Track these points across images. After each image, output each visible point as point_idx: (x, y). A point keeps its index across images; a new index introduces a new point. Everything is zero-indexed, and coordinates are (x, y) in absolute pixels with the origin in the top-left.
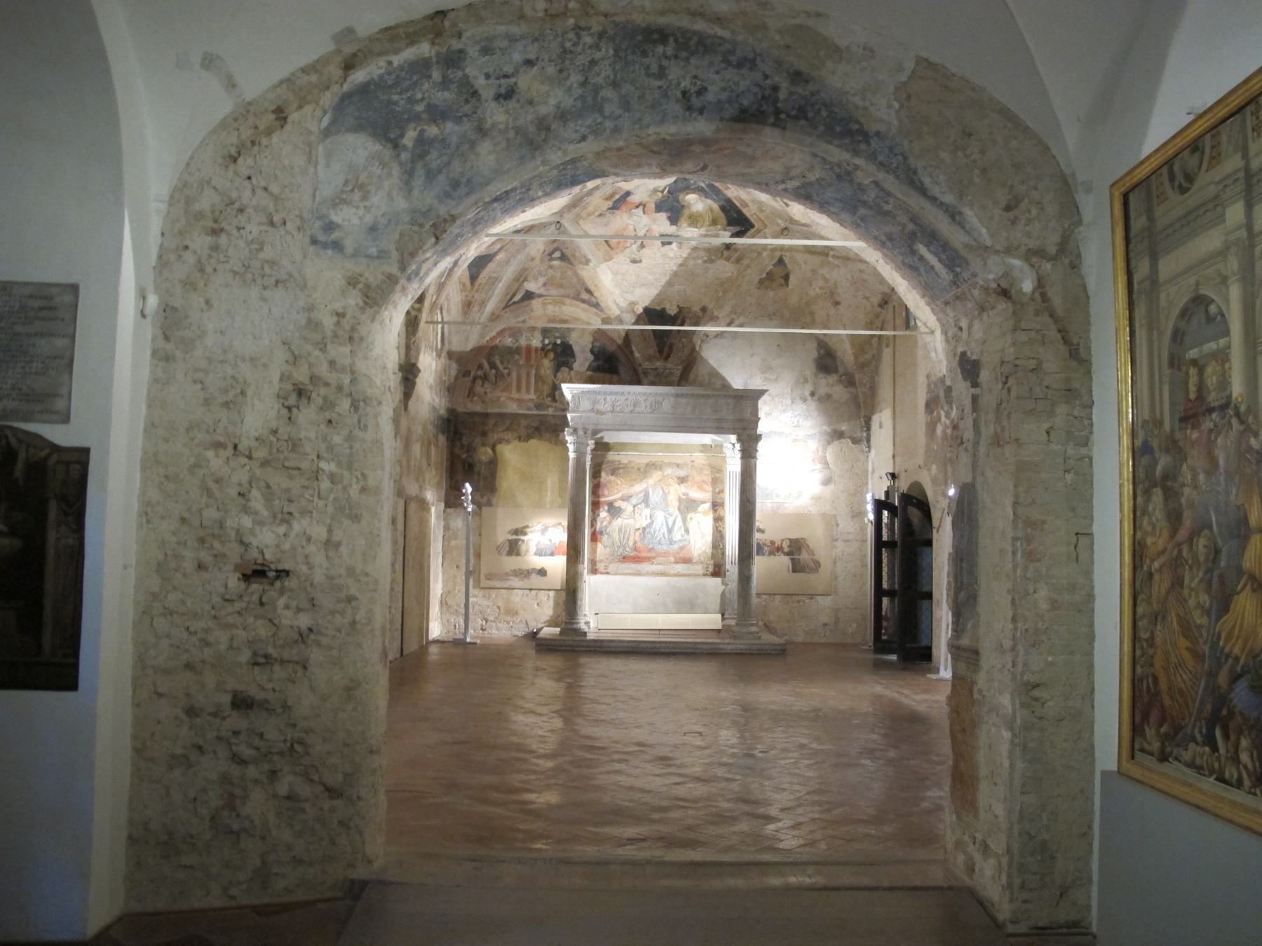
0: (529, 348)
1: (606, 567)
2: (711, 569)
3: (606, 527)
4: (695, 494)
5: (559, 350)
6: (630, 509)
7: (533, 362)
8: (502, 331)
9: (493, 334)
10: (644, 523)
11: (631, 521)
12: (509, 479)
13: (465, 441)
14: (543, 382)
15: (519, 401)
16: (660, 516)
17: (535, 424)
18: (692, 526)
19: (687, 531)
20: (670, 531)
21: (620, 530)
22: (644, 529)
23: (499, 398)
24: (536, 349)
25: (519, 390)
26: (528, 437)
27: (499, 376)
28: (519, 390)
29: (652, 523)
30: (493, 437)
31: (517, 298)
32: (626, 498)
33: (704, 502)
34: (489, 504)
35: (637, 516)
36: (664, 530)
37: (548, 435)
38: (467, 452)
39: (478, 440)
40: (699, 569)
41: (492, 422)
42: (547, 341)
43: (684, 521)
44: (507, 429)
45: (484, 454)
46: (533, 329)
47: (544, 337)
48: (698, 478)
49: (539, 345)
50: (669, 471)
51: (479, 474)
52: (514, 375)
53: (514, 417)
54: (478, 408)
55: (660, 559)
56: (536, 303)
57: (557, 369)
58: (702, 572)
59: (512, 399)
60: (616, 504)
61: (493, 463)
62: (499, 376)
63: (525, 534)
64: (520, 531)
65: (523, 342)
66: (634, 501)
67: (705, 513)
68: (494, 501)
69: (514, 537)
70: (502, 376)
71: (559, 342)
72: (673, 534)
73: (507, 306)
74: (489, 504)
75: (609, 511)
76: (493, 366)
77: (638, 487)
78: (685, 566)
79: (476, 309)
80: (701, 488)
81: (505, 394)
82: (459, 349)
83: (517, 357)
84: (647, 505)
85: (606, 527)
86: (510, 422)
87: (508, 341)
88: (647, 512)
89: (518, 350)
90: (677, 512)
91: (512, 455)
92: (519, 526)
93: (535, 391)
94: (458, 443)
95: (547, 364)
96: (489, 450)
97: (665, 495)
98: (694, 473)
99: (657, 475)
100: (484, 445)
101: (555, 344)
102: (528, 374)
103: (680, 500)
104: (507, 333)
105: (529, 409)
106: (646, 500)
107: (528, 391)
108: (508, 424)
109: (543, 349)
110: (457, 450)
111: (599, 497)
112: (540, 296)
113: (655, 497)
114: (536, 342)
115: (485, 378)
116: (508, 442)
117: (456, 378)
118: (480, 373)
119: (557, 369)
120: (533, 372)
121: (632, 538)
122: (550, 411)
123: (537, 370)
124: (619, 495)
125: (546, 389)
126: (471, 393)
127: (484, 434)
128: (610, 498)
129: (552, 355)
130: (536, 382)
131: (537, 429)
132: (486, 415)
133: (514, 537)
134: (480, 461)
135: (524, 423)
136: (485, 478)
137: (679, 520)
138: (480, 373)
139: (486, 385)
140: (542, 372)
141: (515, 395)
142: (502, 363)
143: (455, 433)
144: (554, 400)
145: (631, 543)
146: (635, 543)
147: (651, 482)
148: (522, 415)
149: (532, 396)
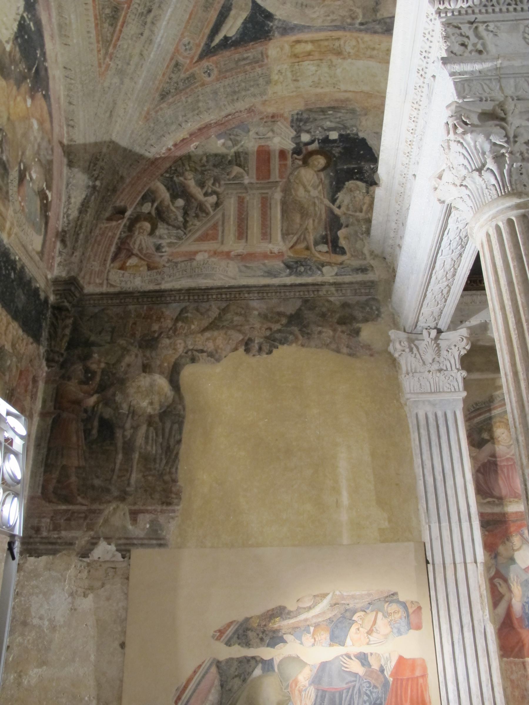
0: (264, 155)
5: (336, 151)
7: (275, 176)
8: (208, 127)
9: (182, 134)
12: (217, 458)
13: (97, 362)
14: (304, 214)
15: (244, 258)
17: (290, 309)
23: (191, 256)
24: (282, 154)
25: (242, 233)
26: (273, 342)
27: (194, 209)
28: (242, 233)
30: (170, 350)
31: (232, 28)
34: (156, 539)
37: (327, 333)
38: (102, 389)
39: (133, 358)
41: (171, 311)
42: (305, 138)
44: (213, 326)
45: (146, 392)
46: (274, 118)
47: (299, 131)
49: (290, 146)
51: (129, 447)
52: (231, 205)
53: (232, 296)
54: (138, 281)
56: (276, 49)
57: (337, 186)
59: (227, 255)
61: (171, 419)
62: (194, 209)
63: (275, 639)
64: (258, 630)
65: (250, 143)
68: (171, 529)
69: (238, 651)
70: (201, 207)
71: (334, 135)
73: (208, 52)
74: (156, 539)
76: (178, 191)
79: (132, 28)
81: (212, 245)
82: (91, 139)
83: (236, 170)
86: (218, 307)
87: (218, 145)
89: (239, 159)
91: (227, 393)
92: (255, 609)
93: (285, 234)
94: (79, 368)
95: (311, 181)
96: (162, 382)
100: (146, 368)
101: (326, 140)
102: (265, 204)
104: (213, 132)
105: (270, 274)
107: (266, 234)
108: (214, 312)
109: (297, 151)
110: (73, 387)
111: (501, 500)
112: (287, 29)
114: (282, 139)
115: (160, 216)
116: (214, 356)
117: (84, 207)
118: (147, 208)
119: (337, 186)
120: (278, 196)
122: (328, 275)
123: (286, 191)
125: (314, 228)
126: (123, 250)
127: (149, 343)
129: (321, 161)
130: (284, 212)
131: (296, 318)
132: (157, 297)
133: (238, 651)
134: (133, 412)
135: (257, 305)
136: (146, 459)
138: (147, 208)
139: (162, 230)
140: (301, 192)
141: (239, 248)
142: (201, 184)
143: (71, 345)
144: (336, 248)
148: (248, 288)
149: (278, 245)
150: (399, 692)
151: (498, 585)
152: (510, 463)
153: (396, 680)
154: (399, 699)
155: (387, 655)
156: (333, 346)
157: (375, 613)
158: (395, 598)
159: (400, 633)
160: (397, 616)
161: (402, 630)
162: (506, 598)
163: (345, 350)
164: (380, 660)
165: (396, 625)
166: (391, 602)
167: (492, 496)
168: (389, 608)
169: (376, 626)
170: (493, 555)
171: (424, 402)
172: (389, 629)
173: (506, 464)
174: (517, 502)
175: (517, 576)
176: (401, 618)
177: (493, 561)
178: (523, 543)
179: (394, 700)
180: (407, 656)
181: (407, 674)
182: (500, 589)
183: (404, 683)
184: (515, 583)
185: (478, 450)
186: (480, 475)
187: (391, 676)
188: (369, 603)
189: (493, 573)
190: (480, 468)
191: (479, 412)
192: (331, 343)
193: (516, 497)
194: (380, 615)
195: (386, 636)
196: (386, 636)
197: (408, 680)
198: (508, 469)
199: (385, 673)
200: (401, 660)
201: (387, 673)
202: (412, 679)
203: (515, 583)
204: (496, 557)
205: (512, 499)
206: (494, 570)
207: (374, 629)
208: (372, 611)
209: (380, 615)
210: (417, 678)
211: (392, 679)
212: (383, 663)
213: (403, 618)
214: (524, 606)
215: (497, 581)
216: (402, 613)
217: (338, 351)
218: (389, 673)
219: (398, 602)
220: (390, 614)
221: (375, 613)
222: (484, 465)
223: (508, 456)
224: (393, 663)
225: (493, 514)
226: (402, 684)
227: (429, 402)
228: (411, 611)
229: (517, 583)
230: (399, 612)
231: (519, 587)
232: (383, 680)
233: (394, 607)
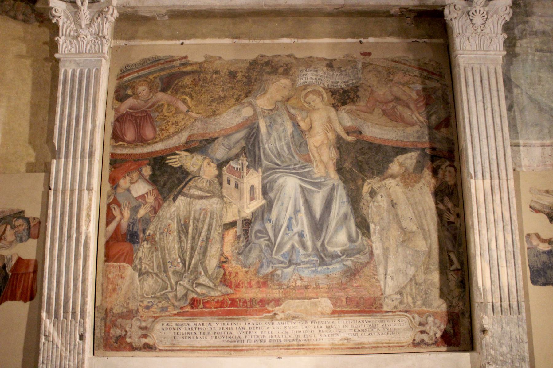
1: (145, 331)
2: (436, 328)
3: (147, 221)
4: (377, 131)
6: (209, 171)
10: (250, 208)
11: (213, 204)
16: (290, 185)
18: (376, 209)
19: (363, 226)
20: (318, 227)
21: (183, 228)
22: (247, 223)
29: (269, 206)
32: (200, 146)
33: (402, 150)
35: (228, 190)
36: (303, 223)
40: (401, 329)
43: (354, 200)
48: (382, 92)
50: (308, 77)
55: (291, 306)
58: (407, 337)
60: (174, 162)
66: (220, 152)
67: (408, 179)
72: (327, 235)
75: (153, 180)
77: (231, 118)
78: (364, 322)
80: (393, 117)
84: (255, 162)
85: (147, 221)
88: (254, 179)
90: (334, 178)
97: (301, 136)
98: (372, 80)
99: (277, 88)
103: (340, 145)
106: (251, 148)
113: (275, 140)
121: (214, 250)
124: (183, 137)
128: (159, 147)
137: (341, 194)
145: (212, 263)
146: (223, 262)
147: (263, 102)
150: (15, 283)
151: (113, 209)
152: (144, 115)
153: (13, 275)
154: (14, 288)
155: (10, 256)
156: (12, 13)
157: (5, 225)
158: (22, 215)
159: (21, 241)
160: (21, 228)
161: (24, 239)
162: (118, 219)
163: (21, 17)
164: (4, 260)
165: (19, 235)
166: (18, 218)
167: (123, 140)
168: (16, 222)
169: (5, 235)
170: (115, 186)
171: (70, 61)
172: (14, 237)
173: (140, 115)
174: (142, 146)
175: (129, 203)
176: (24, 230)
177: (113, 191)
178: (139, 178)
179: (10, 288)
180: (24, 257)
181: (23, 270)
182: (114, 212)
183: (19, 276)
184: (126, 209)
185: (120, 103)
186: (117, 123)
187: (11, 271)
188: (2, 218)
189: (111, 200)
190: (118, 118)
191: (129, 72)
192: (10, 10)
193: (142, 142)
194: (9, 227)
195: (11, 243)
196: (11, 243)
197: (22, 274)
198: (141, 120)
199: (7, 269)
200: (20, 260)
201: (8, 270)
202: (26, 274)
203: (126, 209)
204: (116, 188)
205: (138, 144)
206: (113, 197)
207: (3, 237)
208: (3, 224)
209: (9, 227)
210: (30, 273)
211: (11, 274)
212: (6, 261)
213: (26, 230)
214: (129, 225)
215: (112, 206)
216: (25, 226)
217: (15, 18)
218: (10, 269)
219: (24, 218)
220: (15, 227)
221: (5, 225)
222: (123, 116)
223: (144, 109)
224: (14, 262)
225: (121, 155)
226: (17, 277)
227: (75, 61)
228: (32, 224)
229: (128, 208)
230: (23, 225)
231: (129, 212)
232: (4, 274)
233: (20, 221)
